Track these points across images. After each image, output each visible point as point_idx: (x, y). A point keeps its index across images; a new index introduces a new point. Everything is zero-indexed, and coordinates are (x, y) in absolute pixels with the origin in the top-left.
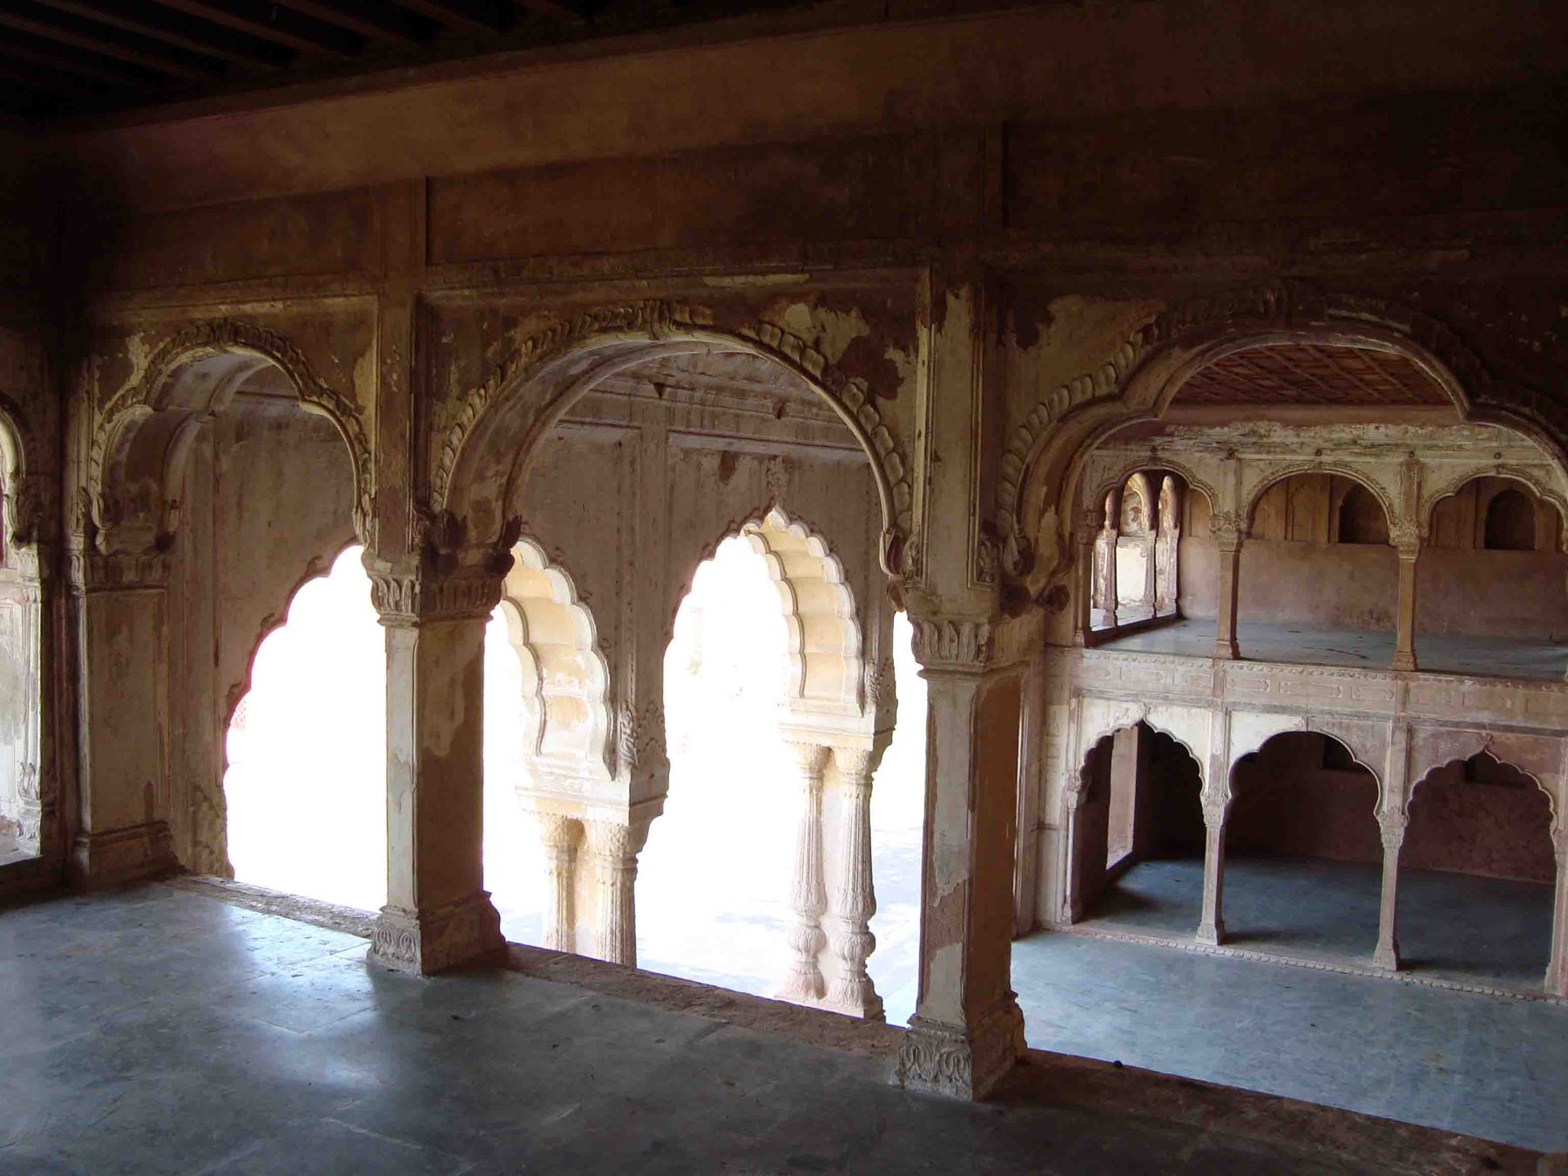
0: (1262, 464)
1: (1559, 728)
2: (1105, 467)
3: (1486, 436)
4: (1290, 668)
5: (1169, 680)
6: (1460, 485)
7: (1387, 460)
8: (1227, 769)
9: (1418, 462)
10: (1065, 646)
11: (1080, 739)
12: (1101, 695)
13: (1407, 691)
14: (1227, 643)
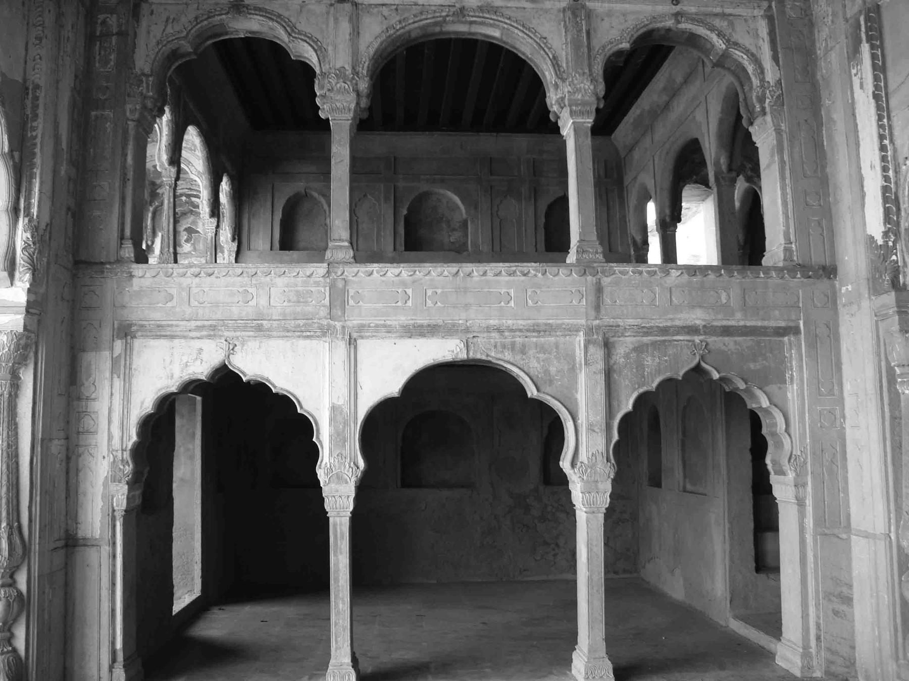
0: (386, 12)
1: (783, 324)
2: (167, 21)
4: (439, 270)
5: (263, 302)
8: (356, 423)
9: (584, 7)
10: (102, 263)
11: (129, 401)
12: (160, 332)
13: (599, 290)
14: (346, 244)
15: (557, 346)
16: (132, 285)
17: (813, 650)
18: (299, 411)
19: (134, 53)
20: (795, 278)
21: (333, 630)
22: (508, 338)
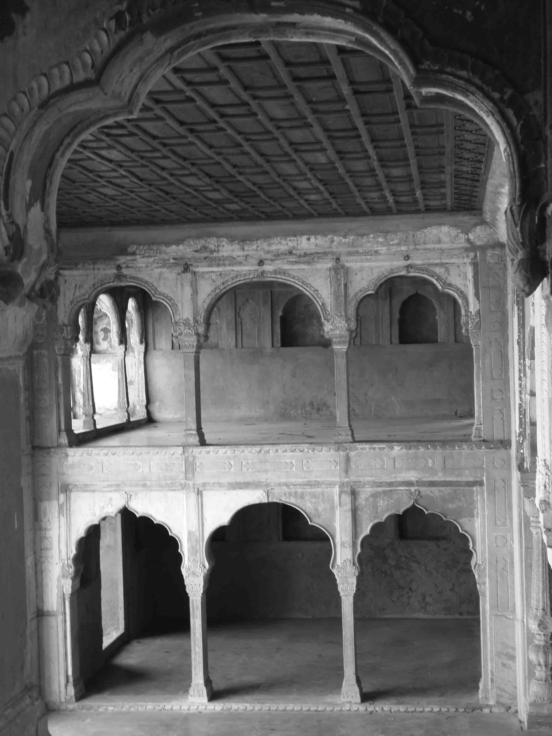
0: (214, 276)
1: (471, 479)
2: (76, 286)
3: (396, 241)
4: (249, 449)
5: (147, 470)
6: (378, 285)
7: (319, 266)
8: (203, 542)
9: (343, 267)
10: (49, 448)
12: (85, 488)
13: (348, 459)
14: (195, 432)
15: (323, 493)
16: (68, 461)
17: (490, 688)
18: (170, 534)
19: (57, 310)
20: (481, 449)
21: (193, 663)
22: (293, 490)
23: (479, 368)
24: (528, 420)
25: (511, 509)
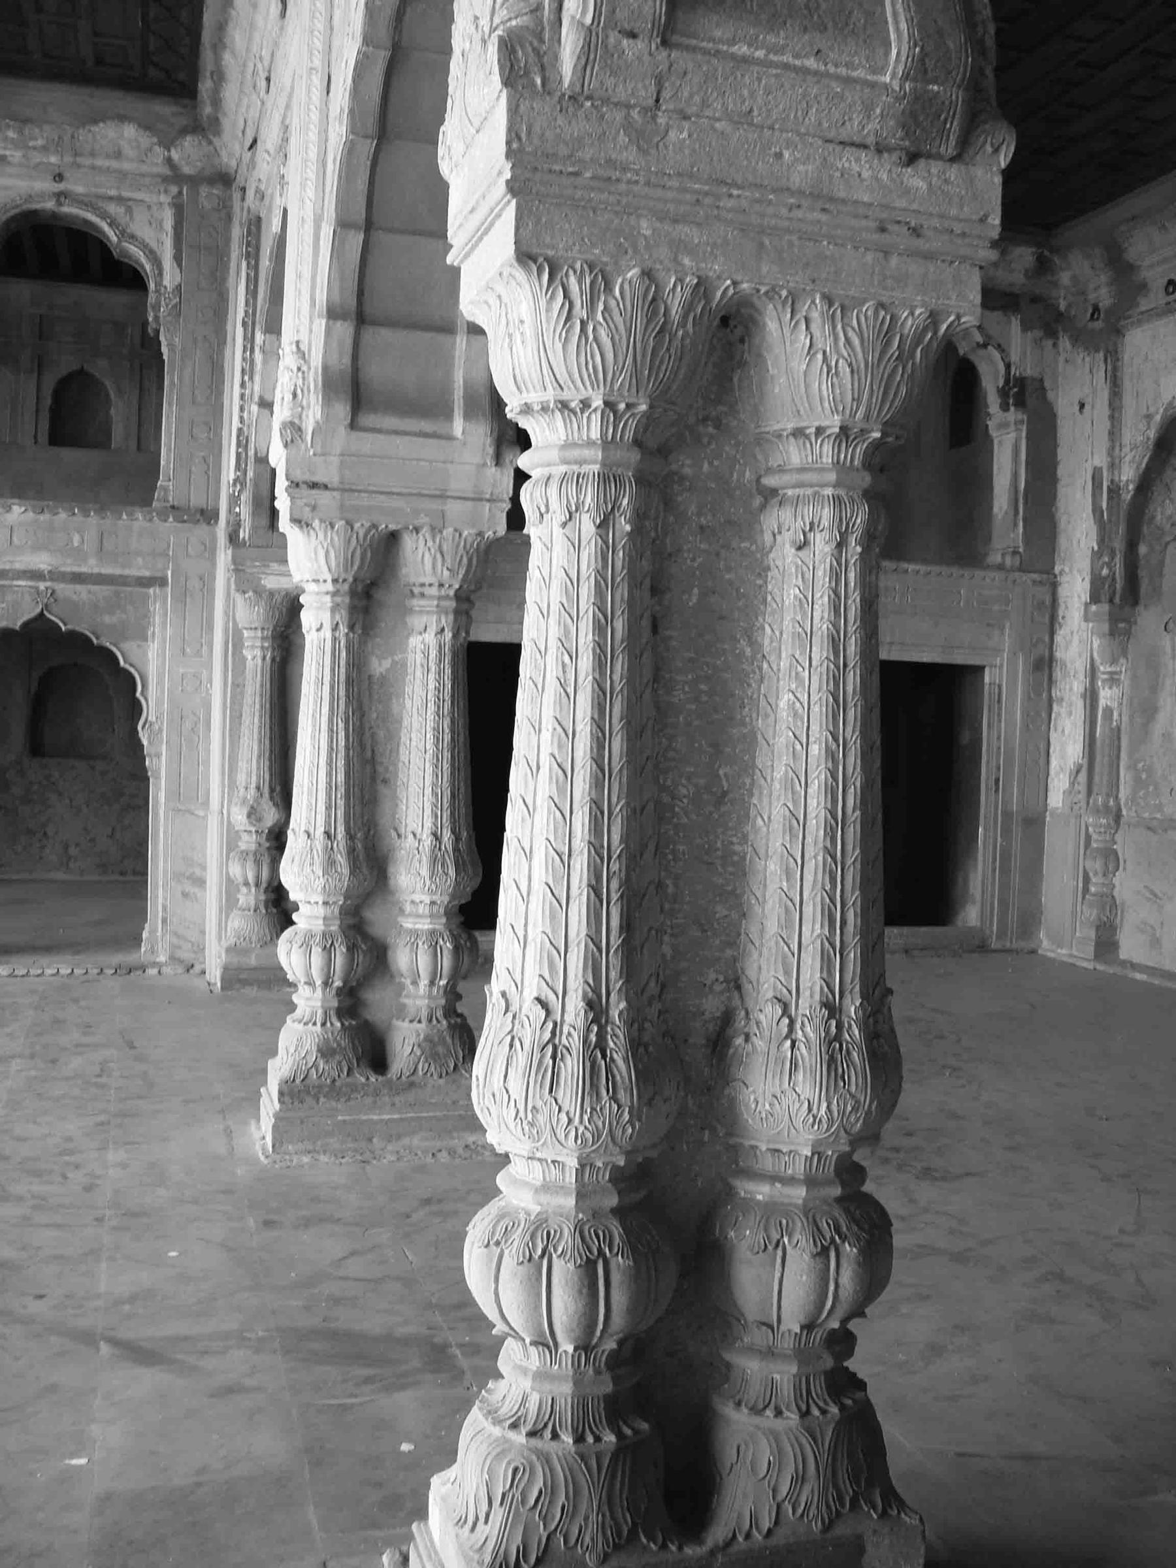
1: (147, 574)
3: (40, 142)
20: (166, 521)
23: (172, 383)
24: (251, 453)
25: (211, 628)
